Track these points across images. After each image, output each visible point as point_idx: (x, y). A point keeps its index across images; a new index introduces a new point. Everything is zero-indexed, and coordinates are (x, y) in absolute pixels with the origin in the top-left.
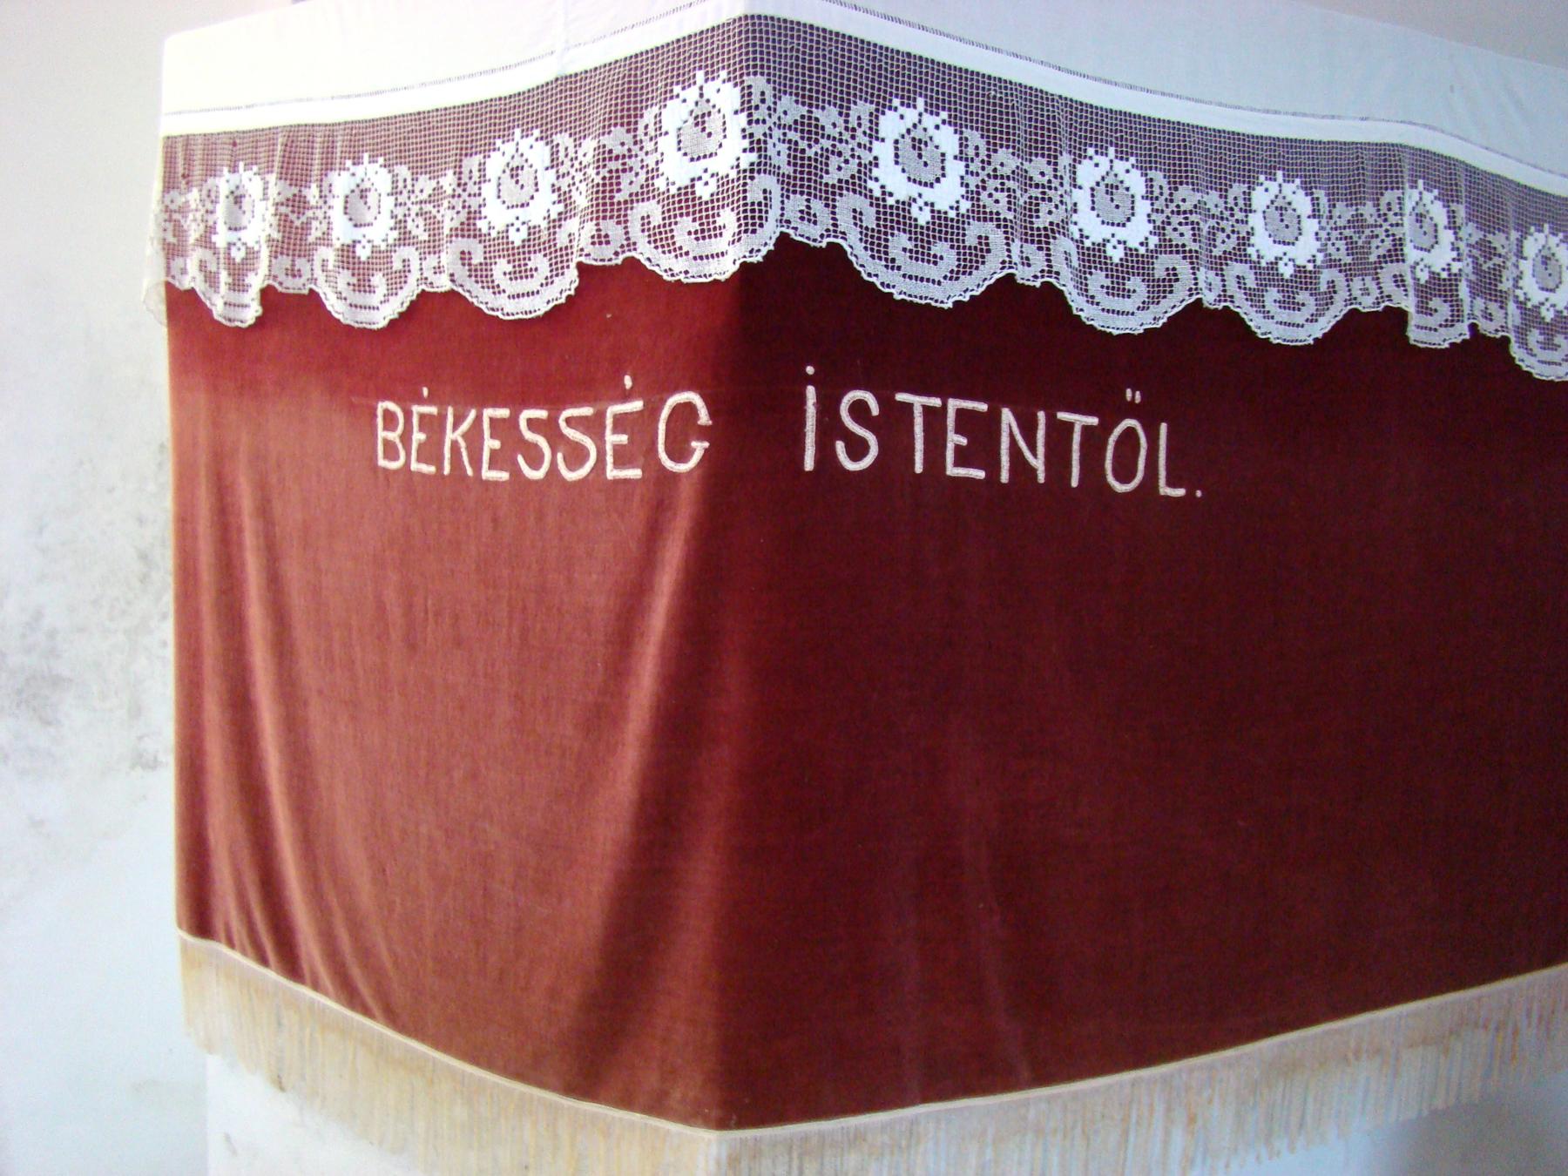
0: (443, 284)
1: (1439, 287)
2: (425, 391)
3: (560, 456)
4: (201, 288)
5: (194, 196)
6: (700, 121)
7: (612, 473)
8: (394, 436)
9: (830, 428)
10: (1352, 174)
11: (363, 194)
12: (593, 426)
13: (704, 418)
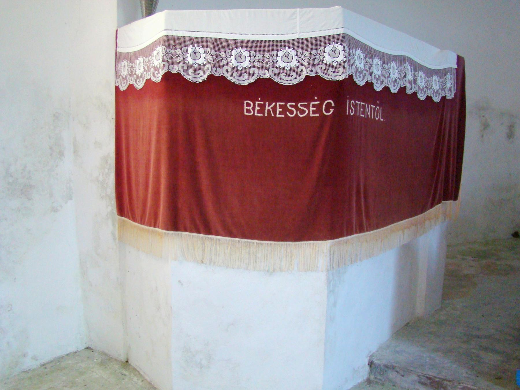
0: (266, 76)
1: (410, 82)
2: (260, 99)
3: (298, 112)
4: (182, 73)
5: (178, 51)
6: (334, 51)
7: (311, 115)
8: (250, 108)
9: (350, 108)
11: (240, 56)
12: (308, 107)
13: (333, 105)
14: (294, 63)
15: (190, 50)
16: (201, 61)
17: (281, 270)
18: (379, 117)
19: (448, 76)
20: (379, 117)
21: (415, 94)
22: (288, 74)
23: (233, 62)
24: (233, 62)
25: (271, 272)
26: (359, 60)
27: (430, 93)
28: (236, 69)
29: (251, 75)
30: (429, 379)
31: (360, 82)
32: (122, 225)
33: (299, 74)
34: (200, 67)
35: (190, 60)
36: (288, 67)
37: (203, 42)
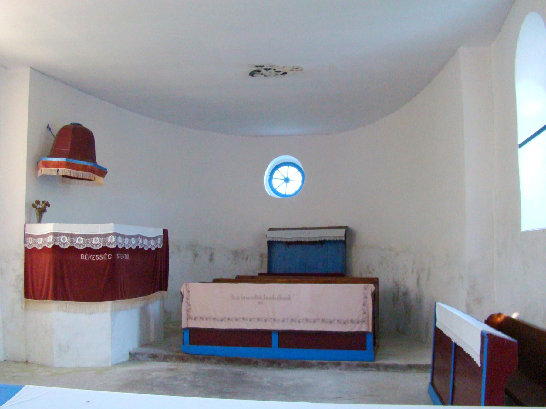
1: (141, 244)
10: (136, 237)
14: (98, 242)
15: (62, 237)
16: (66, 241)
17: (95, 313)
18: (128, 258)
19: (159, 239)
20: (128, 258)
21: (143, 248)
22: (96, 245)
23: (77, 242)
24: (77, 242)
25: (91, 313)
26: (120, 239)
27: (150, 247)
28: (78, 244)
29: (83, 246)
30: (152, 354)
31: (120, 247)
32: (26, 303)
33: (100, 246)
34: (66, 243)
35: (62, 241)
36: (96, 244)
37: (67, 235)
